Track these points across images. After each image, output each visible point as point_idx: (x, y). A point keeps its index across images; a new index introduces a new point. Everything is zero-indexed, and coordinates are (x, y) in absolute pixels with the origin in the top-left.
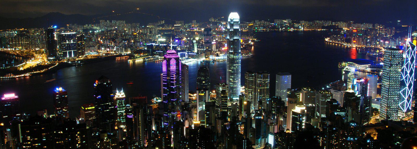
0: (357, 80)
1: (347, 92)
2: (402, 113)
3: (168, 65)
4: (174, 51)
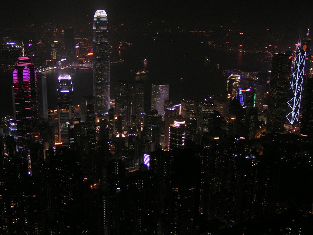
2: (289, 126)
3: (20, 75)
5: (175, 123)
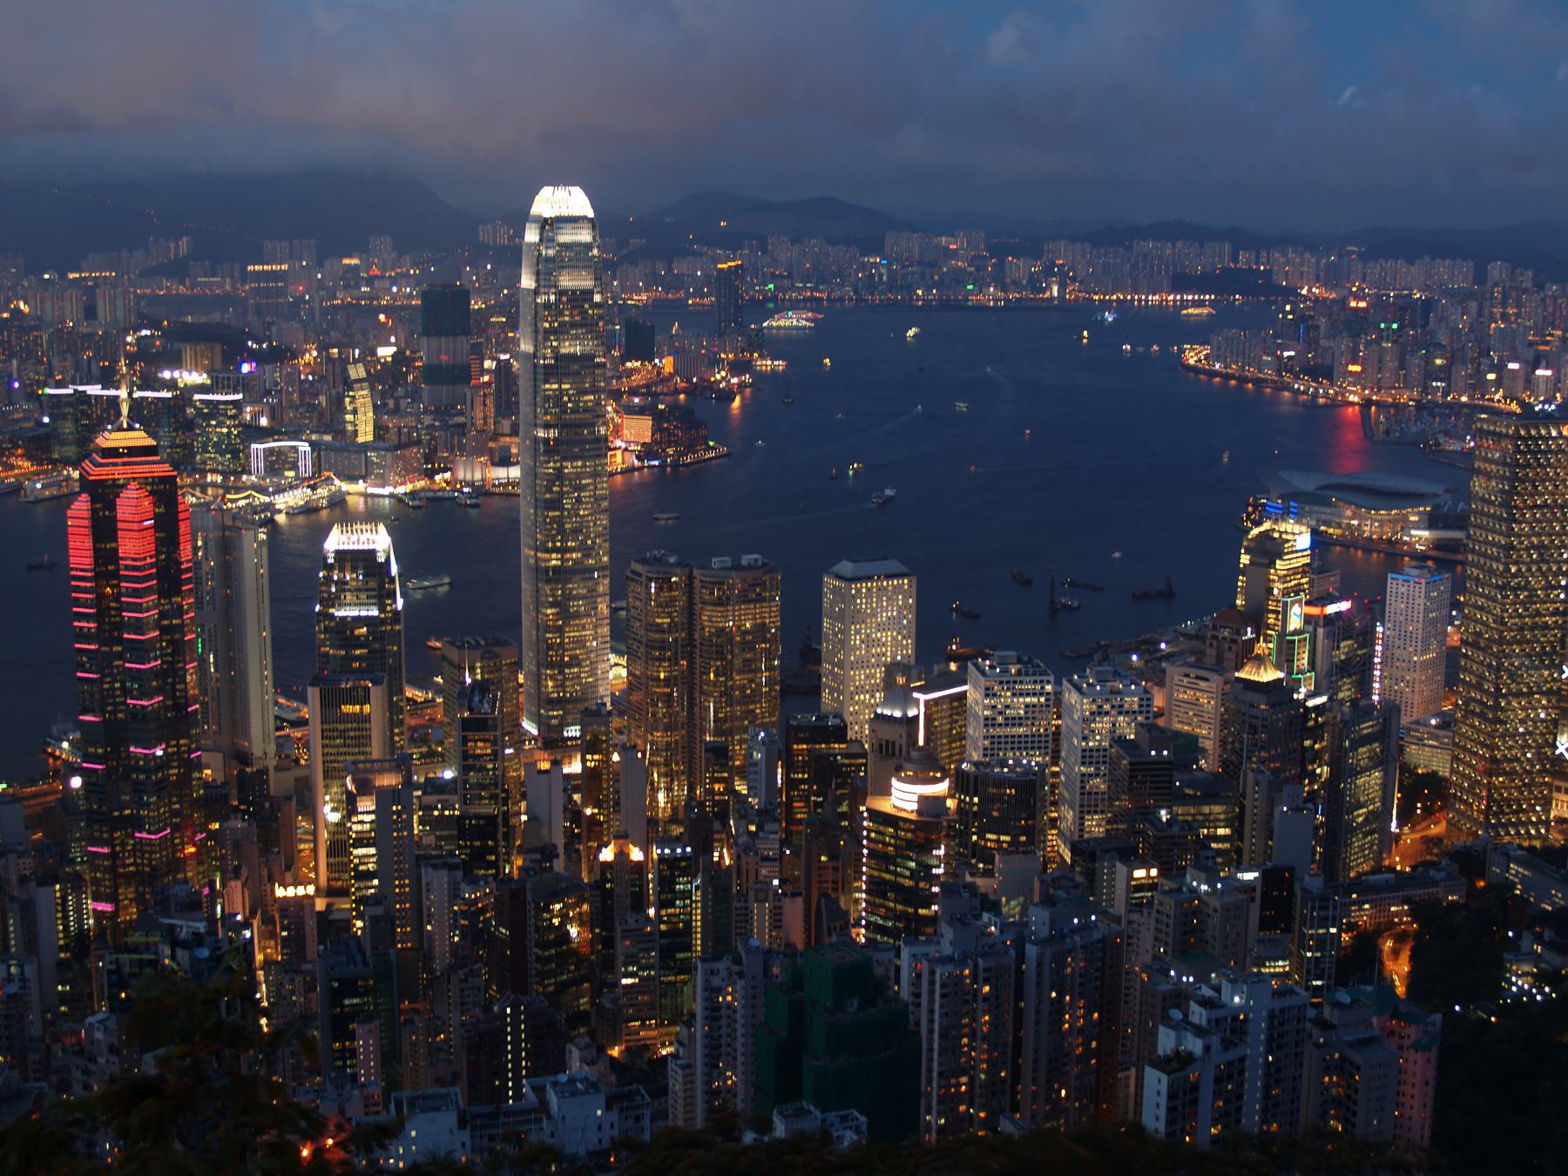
0: (1308, 603)
1: (1239, 679)
3: (104, 529)
4: (145, 435)
5: (893, 791)
